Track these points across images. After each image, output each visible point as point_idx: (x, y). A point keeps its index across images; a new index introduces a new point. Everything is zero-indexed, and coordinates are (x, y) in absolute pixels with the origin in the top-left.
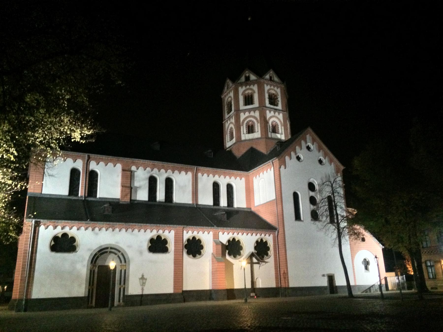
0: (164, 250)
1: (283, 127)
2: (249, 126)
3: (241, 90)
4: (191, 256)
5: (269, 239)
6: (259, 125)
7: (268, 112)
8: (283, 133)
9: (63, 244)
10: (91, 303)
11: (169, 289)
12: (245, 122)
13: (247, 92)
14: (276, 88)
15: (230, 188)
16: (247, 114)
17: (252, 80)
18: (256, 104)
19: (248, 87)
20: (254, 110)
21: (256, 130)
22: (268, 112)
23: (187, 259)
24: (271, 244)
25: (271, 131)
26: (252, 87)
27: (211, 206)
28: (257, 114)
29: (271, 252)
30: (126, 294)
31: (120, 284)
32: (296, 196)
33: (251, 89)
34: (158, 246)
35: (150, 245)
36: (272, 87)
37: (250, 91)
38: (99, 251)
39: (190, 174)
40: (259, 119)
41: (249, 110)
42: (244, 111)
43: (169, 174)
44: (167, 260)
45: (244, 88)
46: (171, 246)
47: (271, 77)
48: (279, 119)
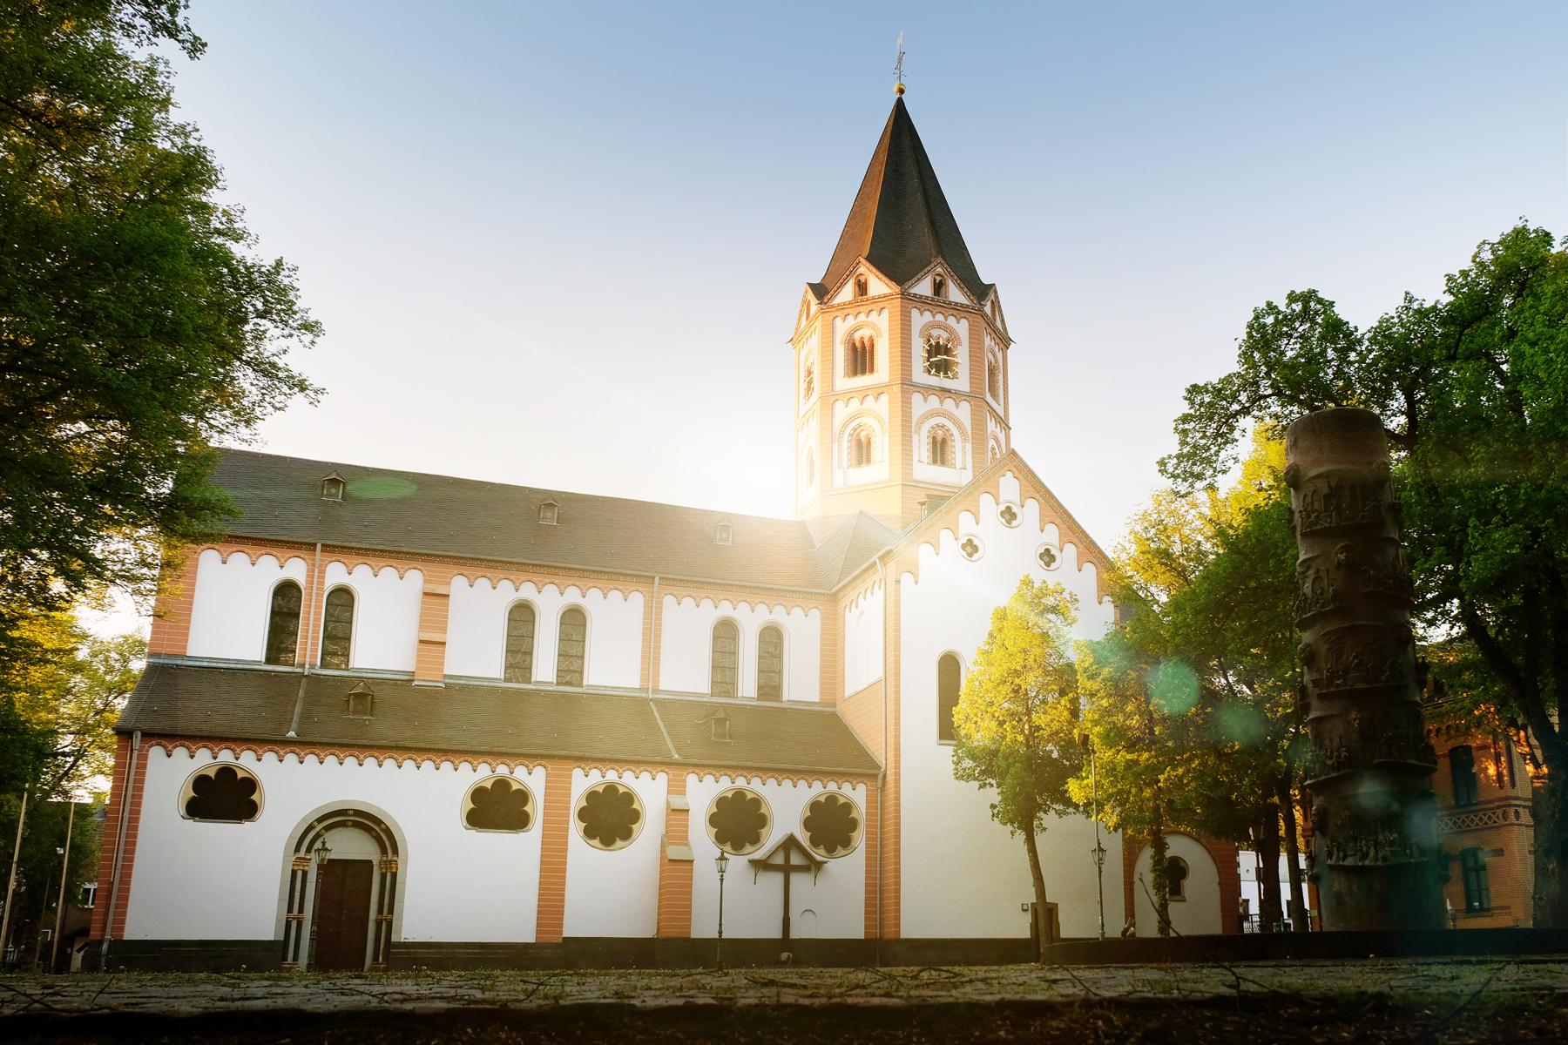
0: (519, 822)
2: (859, 442)
3: (842, 327)
4: (619, 843)
5: (856, 795)
8: (969, 465)
9: (225, 798)
10: (295, 958)
11: (525, 933)
12: (849, 430)
13: (857, 336)
14: (952, 321)
15: (772, 640)
16: (855, 404)
19: (862, 317)
23: (581, 852)
24: (861, 810)
27: (703, 695)
29: (860, 838)
30: (394, 938)
31: (380, 911)
32: (949, 667)
33: (874, 326)
34: (496, 809)
35: (212, 774)
36: (940, 317)
38: (320, 820)
39: (637, 599)
40: (887, 420)
41: (863, 394)
42: (849, 395)
43: (573, 596)
44: (517, 852)
45: (851, 321)
46: (536, 808)
47: (938, 287)
48: (956, 422)
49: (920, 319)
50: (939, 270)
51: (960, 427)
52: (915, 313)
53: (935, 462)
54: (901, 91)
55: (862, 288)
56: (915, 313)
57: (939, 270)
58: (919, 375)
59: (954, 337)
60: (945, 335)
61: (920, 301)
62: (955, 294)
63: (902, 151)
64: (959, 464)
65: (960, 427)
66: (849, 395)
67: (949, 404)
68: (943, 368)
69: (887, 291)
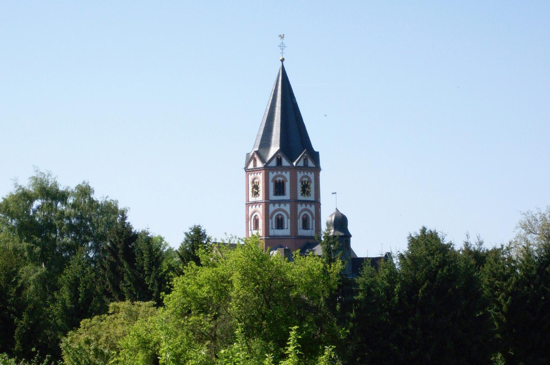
1: (314, 221)
2: (278, 219)
6: (289, 220)
7: (299, 206)
13: (278, 179)
14: (309, 174)
17: (284, 167)
18: (287, 197)
19: (279, 173)
20: (285, 202)
22: (299, 206)
26: (284, 173)
28: (287, 208)
36: (306, 173)
37: (281, 179)
40: (289, 213)
41: (280, 202)
45: (275, 174)
49: (300, 175)
52: (298, 173)
54: (282, 60)
56: (298, 173)
59: (309, 181)
62: (311, 164)
64: (311, 227)
66: (274, 202)
67: (308, 207)
68: (308, 193)
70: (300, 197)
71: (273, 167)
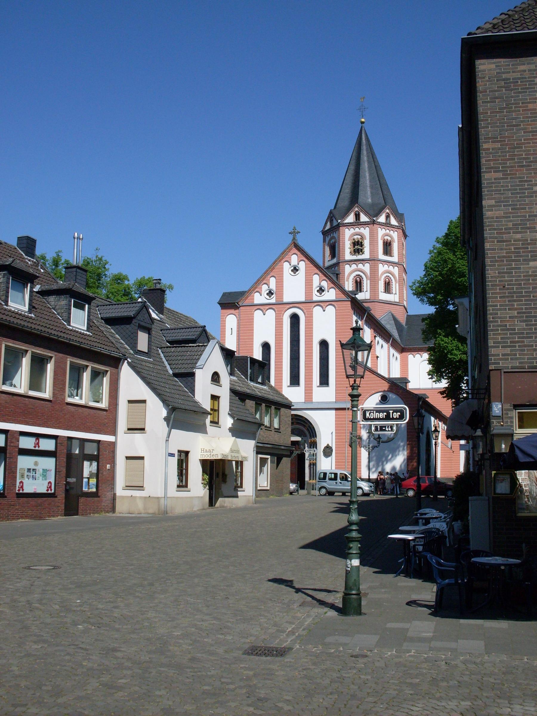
1: (397, 284)
7: (380, 265)
19: (357, 230)
21: (365, 290)
22: (380, 265)
25: (383, 291)
36: (388, 231)
49: (381, 232)
50: (388, 211)
51: (395, 277)
53: (385, 292)
55: (357, 216)
56: (379, 229)
57: (388, 211)
58: (381, 256)
60: (359, 237)
61: (380, 224)
62: (393, 222)
63: (360, 146)
64: (394, 293)
65: (395, 277)
69: (369, 220)
70: (381, 256)
71: (351, 223)
